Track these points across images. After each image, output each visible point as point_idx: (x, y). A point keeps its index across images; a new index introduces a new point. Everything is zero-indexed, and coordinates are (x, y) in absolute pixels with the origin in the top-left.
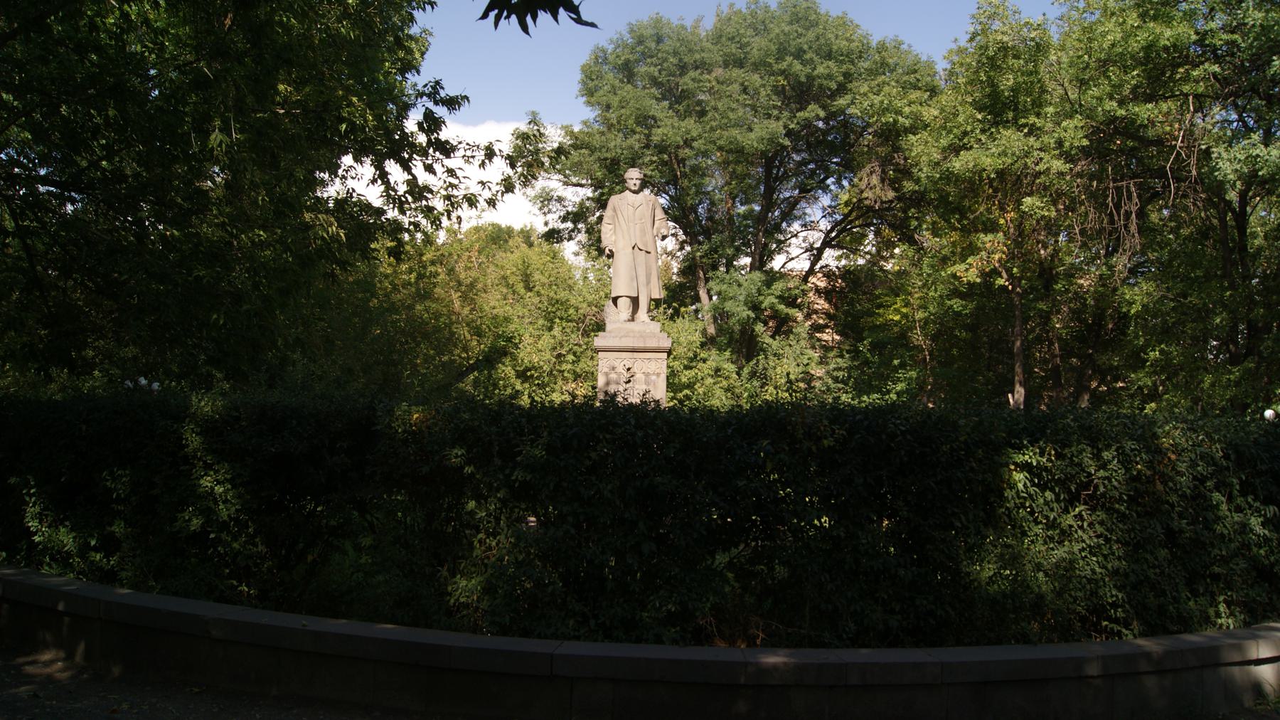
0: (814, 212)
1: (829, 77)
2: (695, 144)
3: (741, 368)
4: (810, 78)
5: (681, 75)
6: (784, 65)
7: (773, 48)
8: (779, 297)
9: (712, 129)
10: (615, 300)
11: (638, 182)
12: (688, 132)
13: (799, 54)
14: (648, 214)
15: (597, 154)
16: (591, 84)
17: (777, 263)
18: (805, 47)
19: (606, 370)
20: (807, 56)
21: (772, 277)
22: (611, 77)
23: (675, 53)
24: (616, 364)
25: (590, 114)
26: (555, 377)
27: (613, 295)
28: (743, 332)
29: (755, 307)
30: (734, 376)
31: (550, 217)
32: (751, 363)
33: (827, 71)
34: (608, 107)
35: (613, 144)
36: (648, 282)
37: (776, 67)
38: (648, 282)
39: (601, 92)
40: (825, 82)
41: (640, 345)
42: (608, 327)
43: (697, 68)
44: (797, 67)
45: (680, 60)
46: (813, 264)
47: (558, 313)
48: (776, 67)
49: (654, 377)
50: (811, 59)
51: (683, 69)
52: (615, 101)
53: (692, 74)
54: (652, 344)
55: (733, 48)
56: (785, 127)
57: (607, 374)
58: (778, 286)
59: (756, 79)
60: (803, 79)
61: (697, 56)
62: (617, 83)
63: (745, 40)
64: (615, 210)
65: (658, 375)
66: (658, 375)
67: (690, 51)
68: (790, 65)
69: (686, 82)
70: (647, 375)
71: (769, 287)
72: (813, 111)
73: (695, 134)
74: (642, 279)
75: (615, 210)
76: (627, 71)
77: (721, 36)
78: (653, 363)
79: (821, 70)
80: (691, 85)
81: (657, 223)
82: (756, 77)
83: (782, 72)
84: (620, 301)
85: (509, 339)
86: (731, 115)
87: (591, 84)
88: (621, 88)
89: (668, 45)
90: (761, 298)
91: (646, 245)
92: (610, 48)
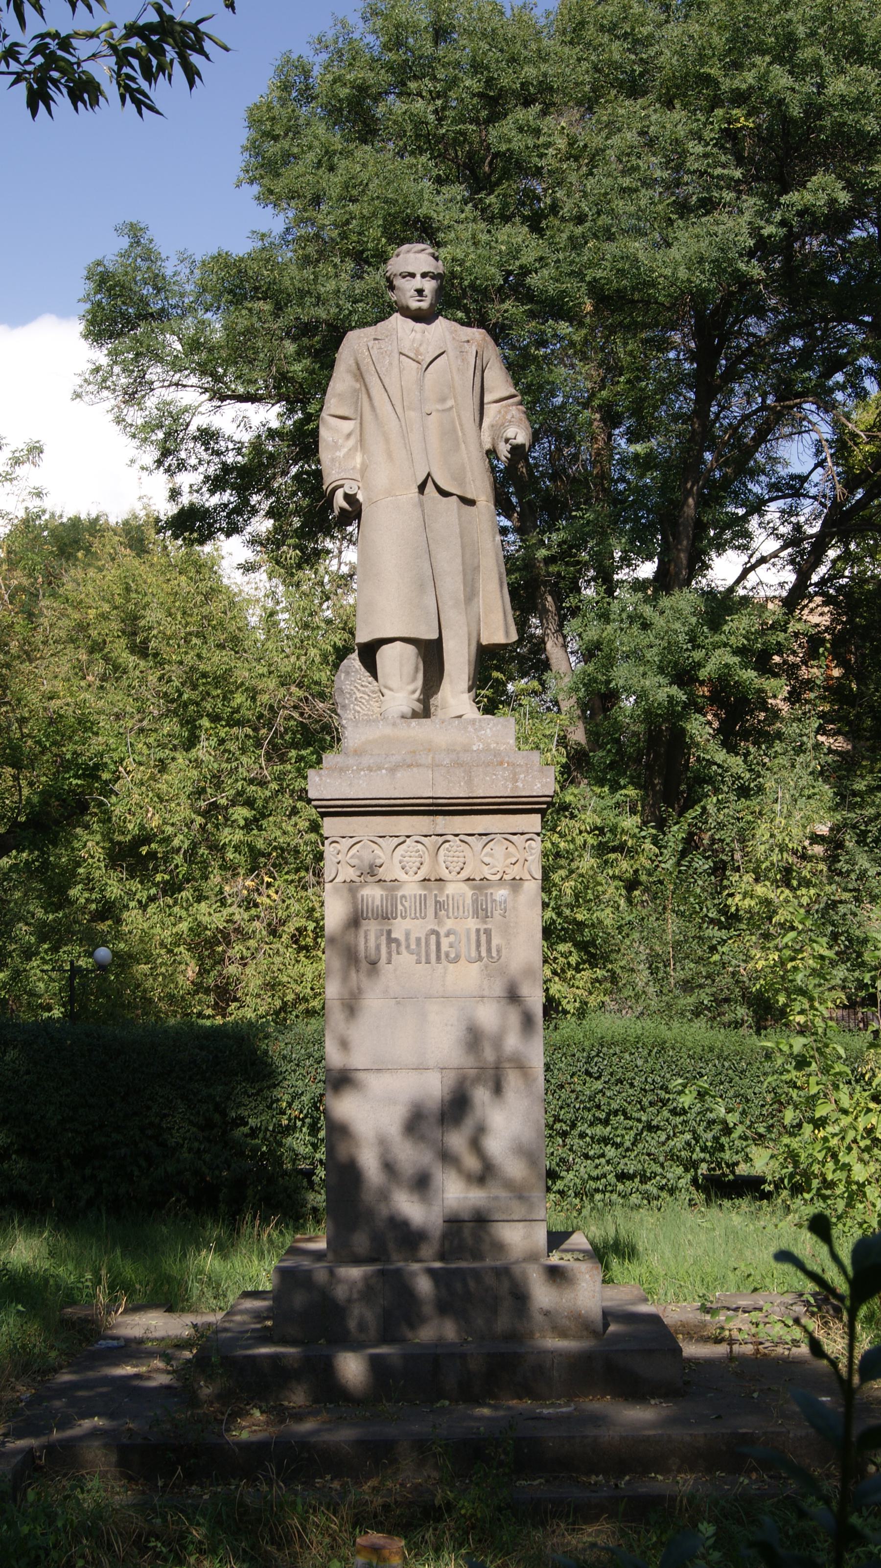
0: (796, 454)
1: (859, 104)
2: (533, 280)
3: (661, 825)
4: (815, 110)
5: (491, 120)
6: (748, 79)
7: (719, 40)
8: (739, 651)
9: (575, 244)
10: (369, 653)
11: (429, 286)
12: (514, 253)
13: (785, 50)
14: (465, 382)
15: (293, 312)
16: (272, 149)
17: (723, 569)
18: (801, 31)
19: (350, 874)
20: (807, 54)
21: (721, 606)
22: (322, 132)
23: (477, 67)
24: (381, 855)
25: (274, 222)
26: (205, 865)
27: (362, 637)
28: (653, 737)
29: (684, 676)
30: (648, 845)
31: (185, 479)
32: (691, 814)
33: (854, 91)
34: (316, 201)
35: (331, 285)
36: (471, 594)
37: (726, 84)
38: (471, 594)
39: (300, 168)
40: (850, 118)
41: (453, 788)
42: (353, 735)
43: (527, 103)
44: (781, 79)
45: (490, 82)
46: (803, 575)
47: (208, 706)
48: (726, 84)
49: (501, 893)
50: (816, 64)
51: (494, 104)
52: (332, 184)
53: (522, 115)
54: (492, 785)
55: (616, 50)
56: (755, 231)
57: (352, 887)
58: (739, 625)
59: (675, 122)
60: (796, 112)
61: (530, 72)
62: (337, 141)
63: (646, 31)
64: (359, 374)
65: (516, 883)
66: (516, 883)
67: (513, 60)
68: (764, 77)
69: (506, 135)
70: (479, 884)
71: (715, 625)
72: (823, 190)
73: (528, 258)
74: (452, 585)
75: (359, 374)
76: (357, 114)
77: (582, 24)
78: (498, 848)
79: (838, 86)
80: (519, 142)
81: (491, 411)
82: (678, 114)
83: (740, 98)
84: (386, 656)
85: (92, 772)
86: (619, 205)
87: (272, 149)
88: (347, 154)
89: (463, 49)
90: (698, 655)
91: (460, 480)
92: (317, 62)
